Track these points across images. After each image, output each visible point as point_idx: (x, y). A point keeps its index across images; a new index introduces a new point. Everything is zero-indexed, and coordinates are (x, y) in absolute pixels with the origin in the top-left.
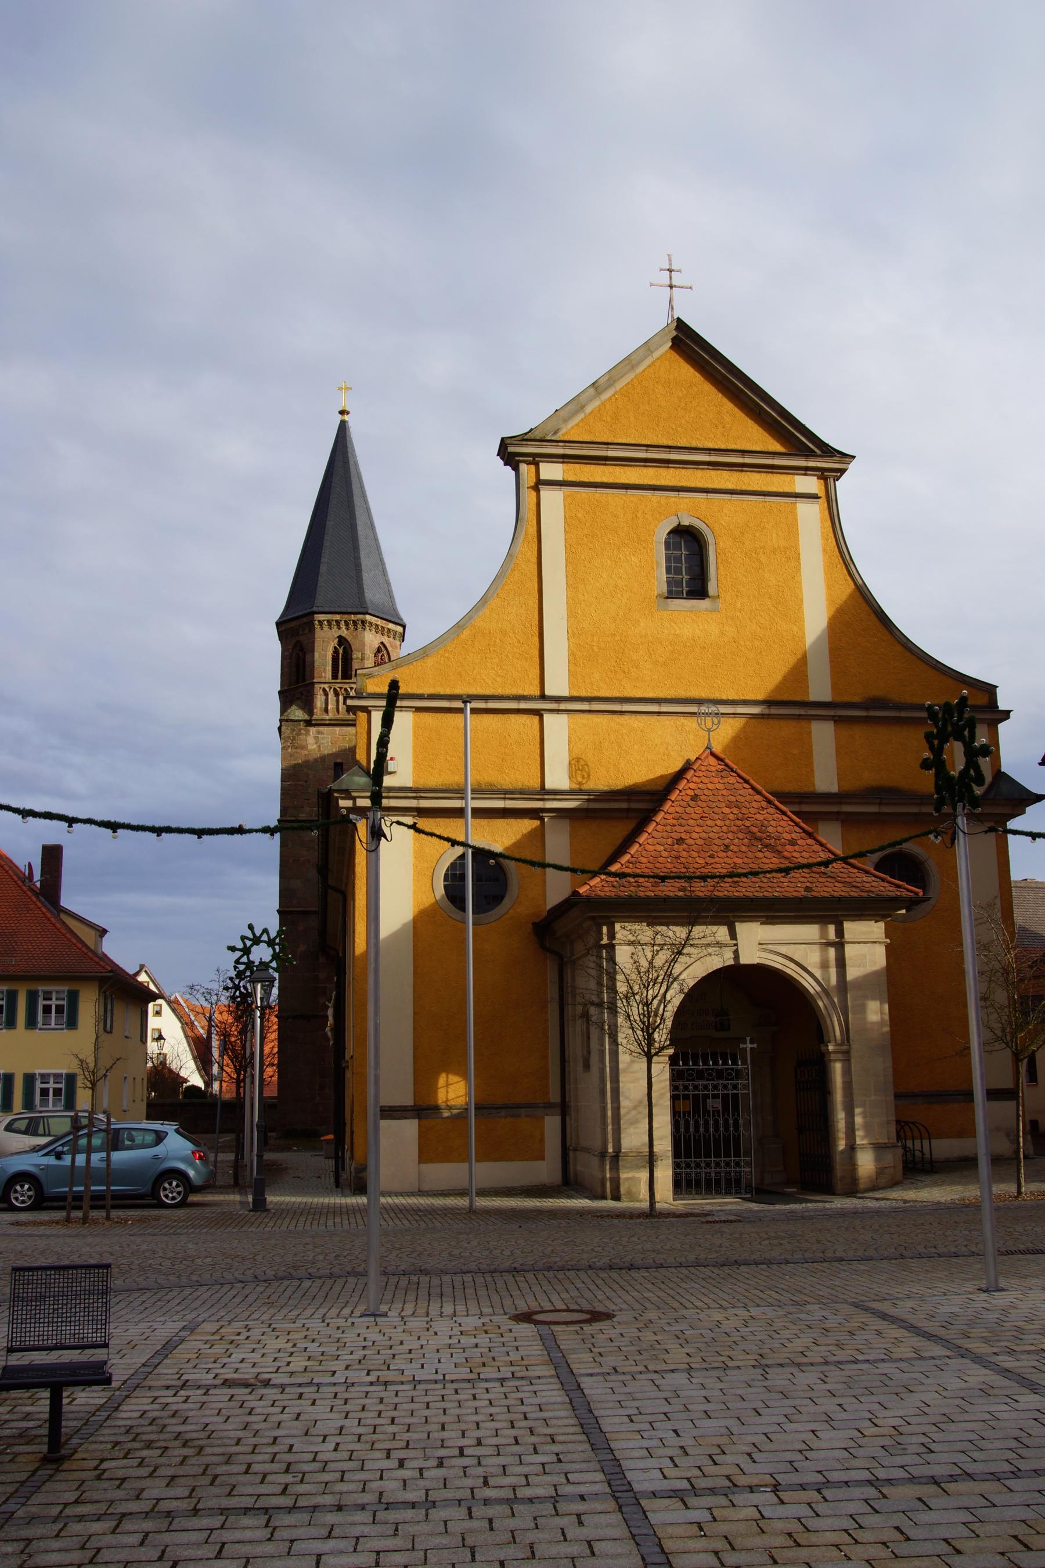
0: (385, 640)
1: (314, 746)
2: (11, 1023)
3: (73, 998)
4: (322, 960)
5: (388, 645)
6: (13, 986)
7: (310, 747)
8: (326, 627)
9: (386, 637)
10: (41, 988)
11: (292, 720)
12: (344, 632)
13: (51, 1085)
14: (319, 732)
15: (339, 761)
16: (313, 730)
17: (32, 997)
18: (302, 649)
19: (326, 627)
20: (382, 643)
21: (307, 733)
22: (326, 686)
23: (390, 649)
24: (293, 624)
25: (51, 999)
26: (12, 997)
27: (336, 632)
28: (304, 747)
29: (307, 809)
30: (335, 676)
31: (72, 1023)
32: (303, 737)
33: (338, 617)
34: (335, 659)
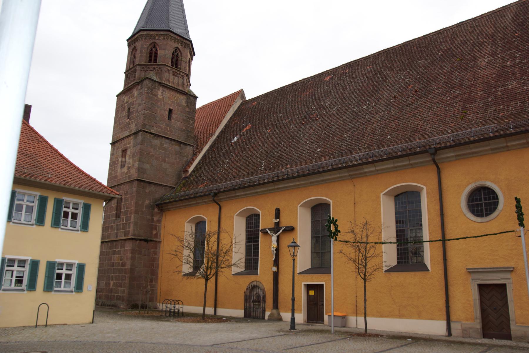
1: (161, 97)
2: (40, 221)
3: (87, 209)
4: (156, 210)
6: (45, 193)
7: (159, 96)
10: (66, 198)
11: (153, 80)
12: (180, 47)
13: (64, 272)
14: (163, 91)
15: (171, 108)
16: (161, 89)
17: (59, 203)
18: (154, 47)
21: (159, 89)
25: (69, 208)
26: (43, 202)
28: (156, 96)
29: (155, 128)
31: (85, 227)
32: (156, 90)
33: (179, 38)
34: (172, 57)
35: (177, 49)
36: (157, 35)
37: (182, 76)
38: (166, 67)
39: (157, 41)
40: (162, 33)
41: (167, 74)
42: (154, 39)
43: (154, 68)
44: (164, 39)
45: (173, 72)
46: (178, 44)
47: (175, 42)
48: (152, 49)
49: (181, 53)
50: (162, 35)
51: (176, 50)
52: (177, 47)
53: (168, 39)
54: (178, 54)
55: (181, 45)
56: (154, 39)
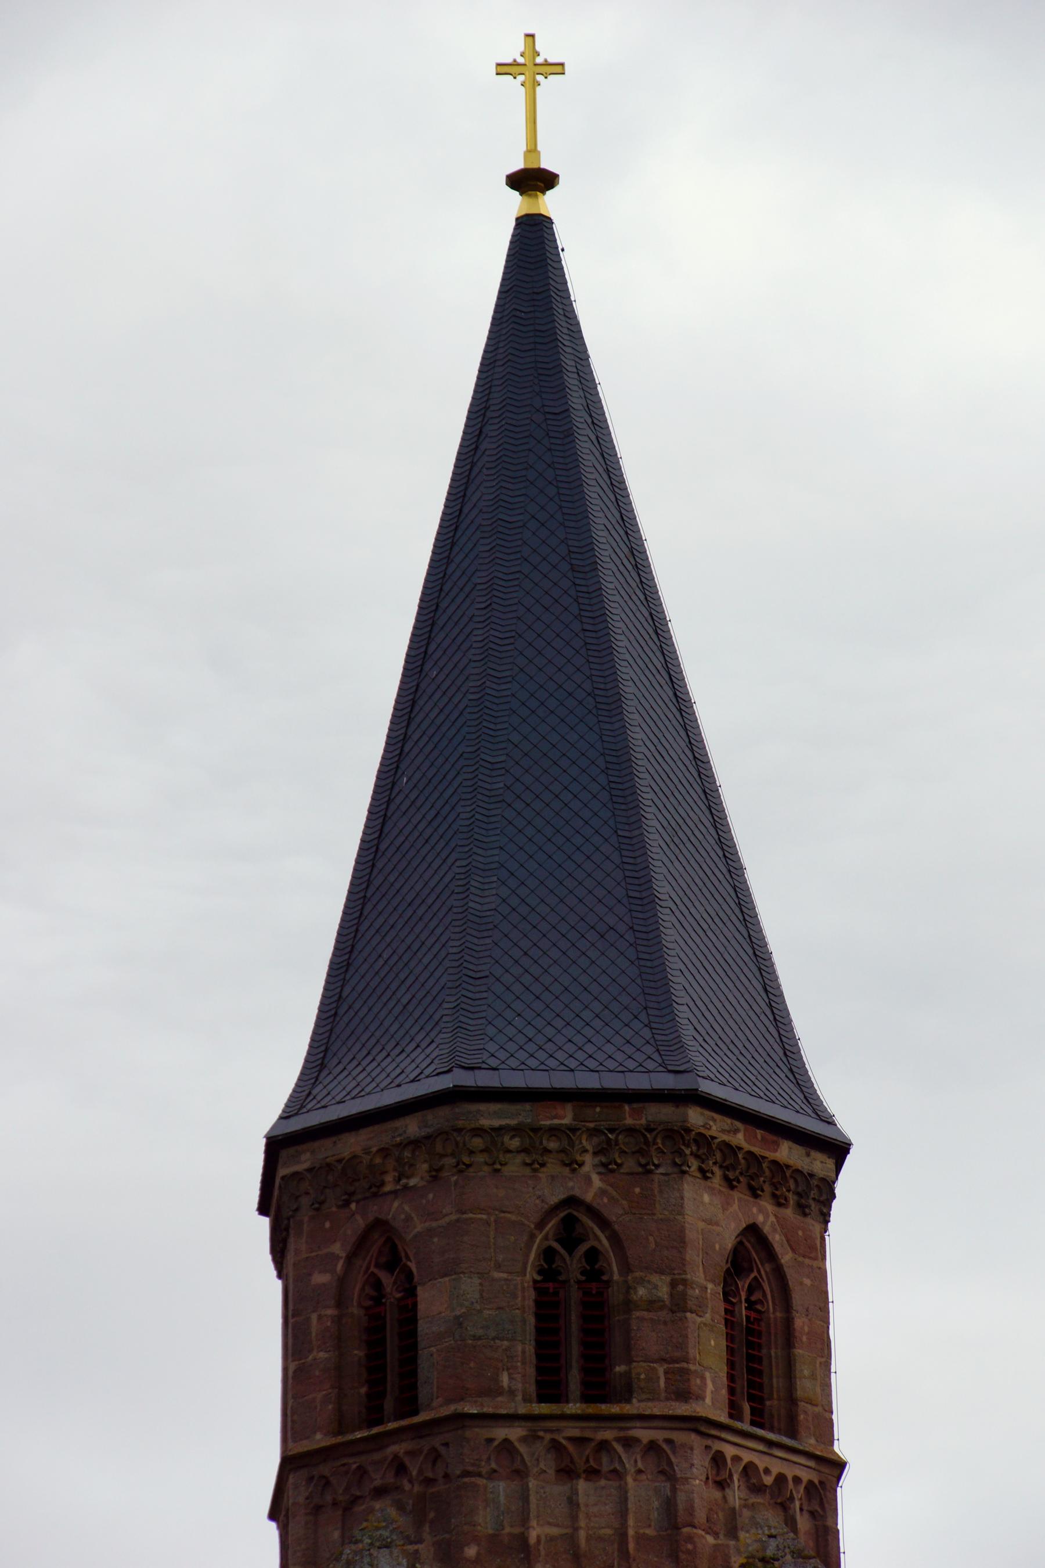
0: (765, 1214)
5: (776, 1239)
8: (514, 1167)
9: (770, 1207)
12: (592, 1184)
19: (514, 1167)
20: (753, 1230)
22: (514, 1433)
23: (786, 1258)
24: (351, 1144)
27: (551, 1188)
30: (549, 1388)
33: (566, 1116)
35: (571, 1220)
36: (385, 1152)
37: (652, 1446)
38: (480, 1433)
39: (395, 1210)
40: (412, 1127)
41: (502, 1489)
42: (375, 1191)
43: (400, 1468)
44: (435, 1175)
45: (556, 1447)
46: (573, 1165)
47: (535, 1166)
48: (378, 1285)
49: (615, 1240)
50: (415, 1144)
51: (569, 1223)
52: (572, 1201)
53: (461, 1168)
54: (593, 1255)
55: (607, 1169)
56: (375, 1191)
